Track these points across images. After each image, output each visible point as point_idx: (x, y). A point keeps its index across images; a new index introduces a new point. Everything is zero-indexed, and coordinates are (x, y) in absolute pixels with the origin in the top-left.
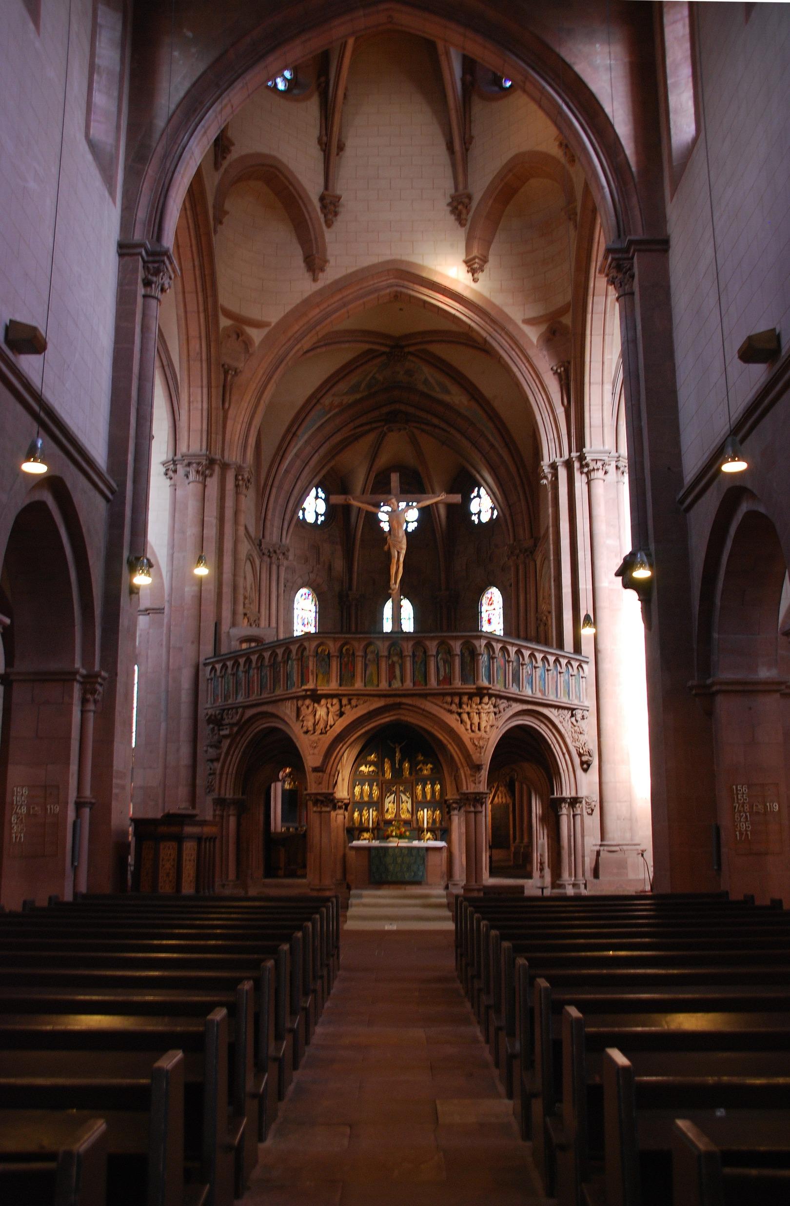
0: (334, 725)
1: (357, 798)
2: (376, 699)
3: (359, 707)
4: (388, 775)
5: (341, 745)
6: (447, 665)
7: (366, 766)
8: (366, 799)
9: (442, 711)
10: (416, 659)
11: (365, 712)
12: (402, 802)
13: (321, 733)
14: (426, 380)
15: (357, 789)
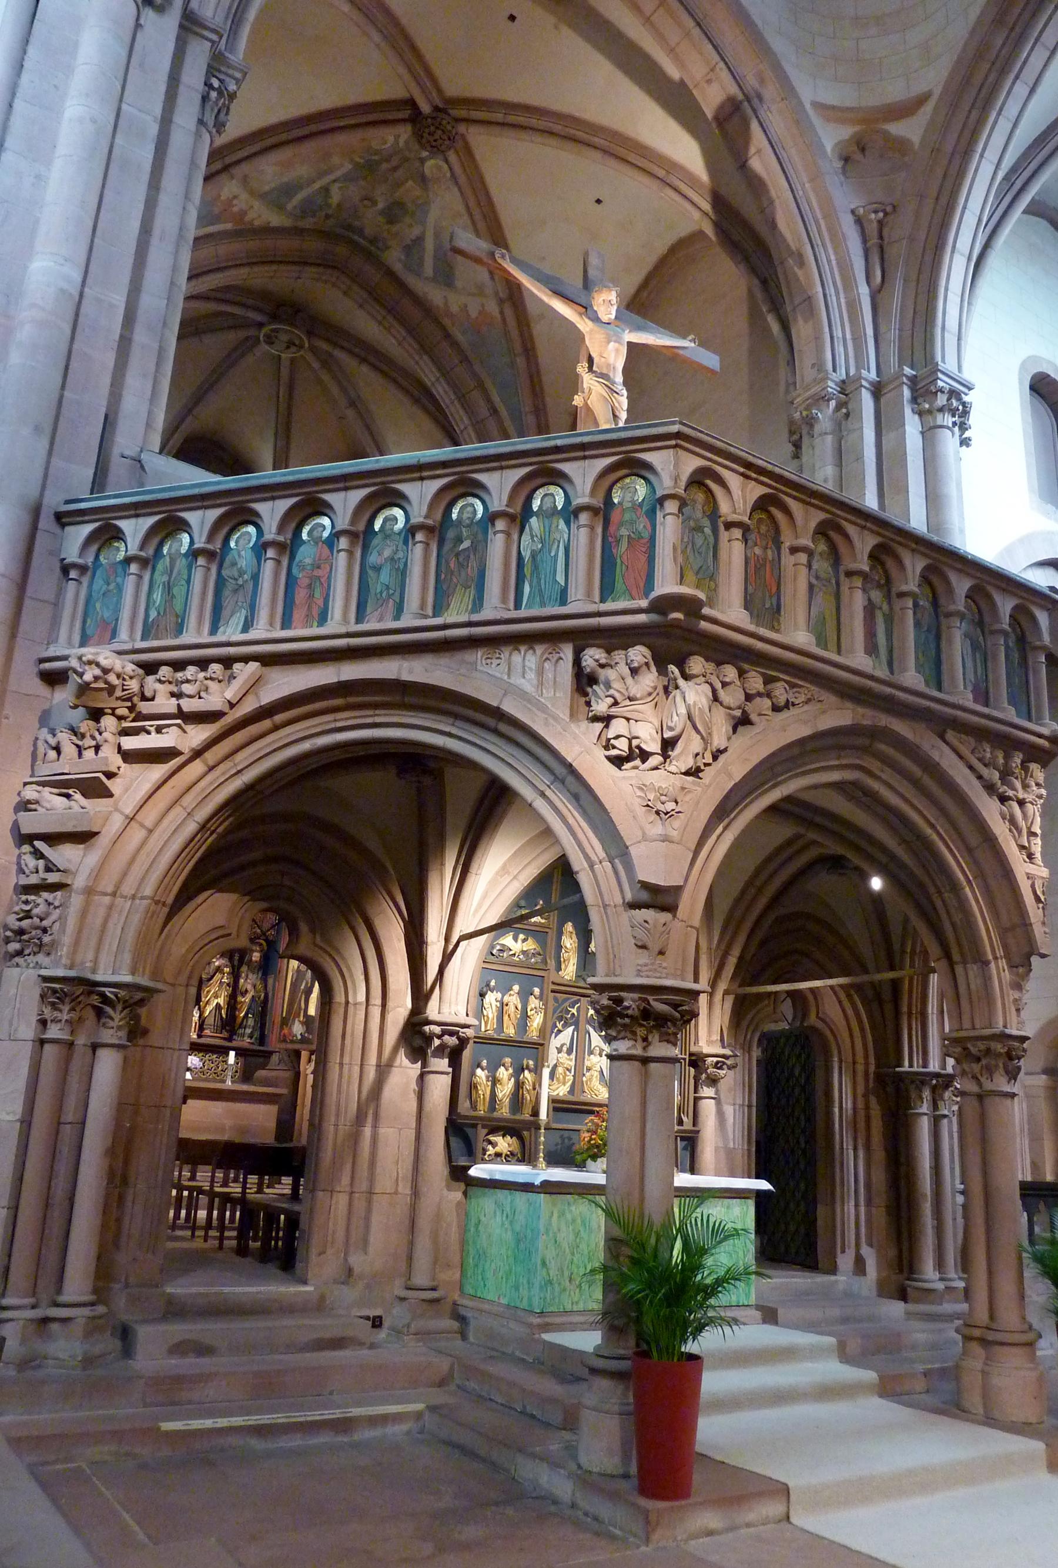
0: (725, 750)
1: (488, 1027)
2: (830, 699)
3: (793, 711)
4: (569, 971)
5: (720, 828)
6: (978, 655)
7: (516, 939)
8: (510, 1031)
9: (976, 783)
10: (919, 615)
11: (805, 731)
12: (591, 1053)
13: (687, 773)
14: (420, 240)
15: (492, 999)
